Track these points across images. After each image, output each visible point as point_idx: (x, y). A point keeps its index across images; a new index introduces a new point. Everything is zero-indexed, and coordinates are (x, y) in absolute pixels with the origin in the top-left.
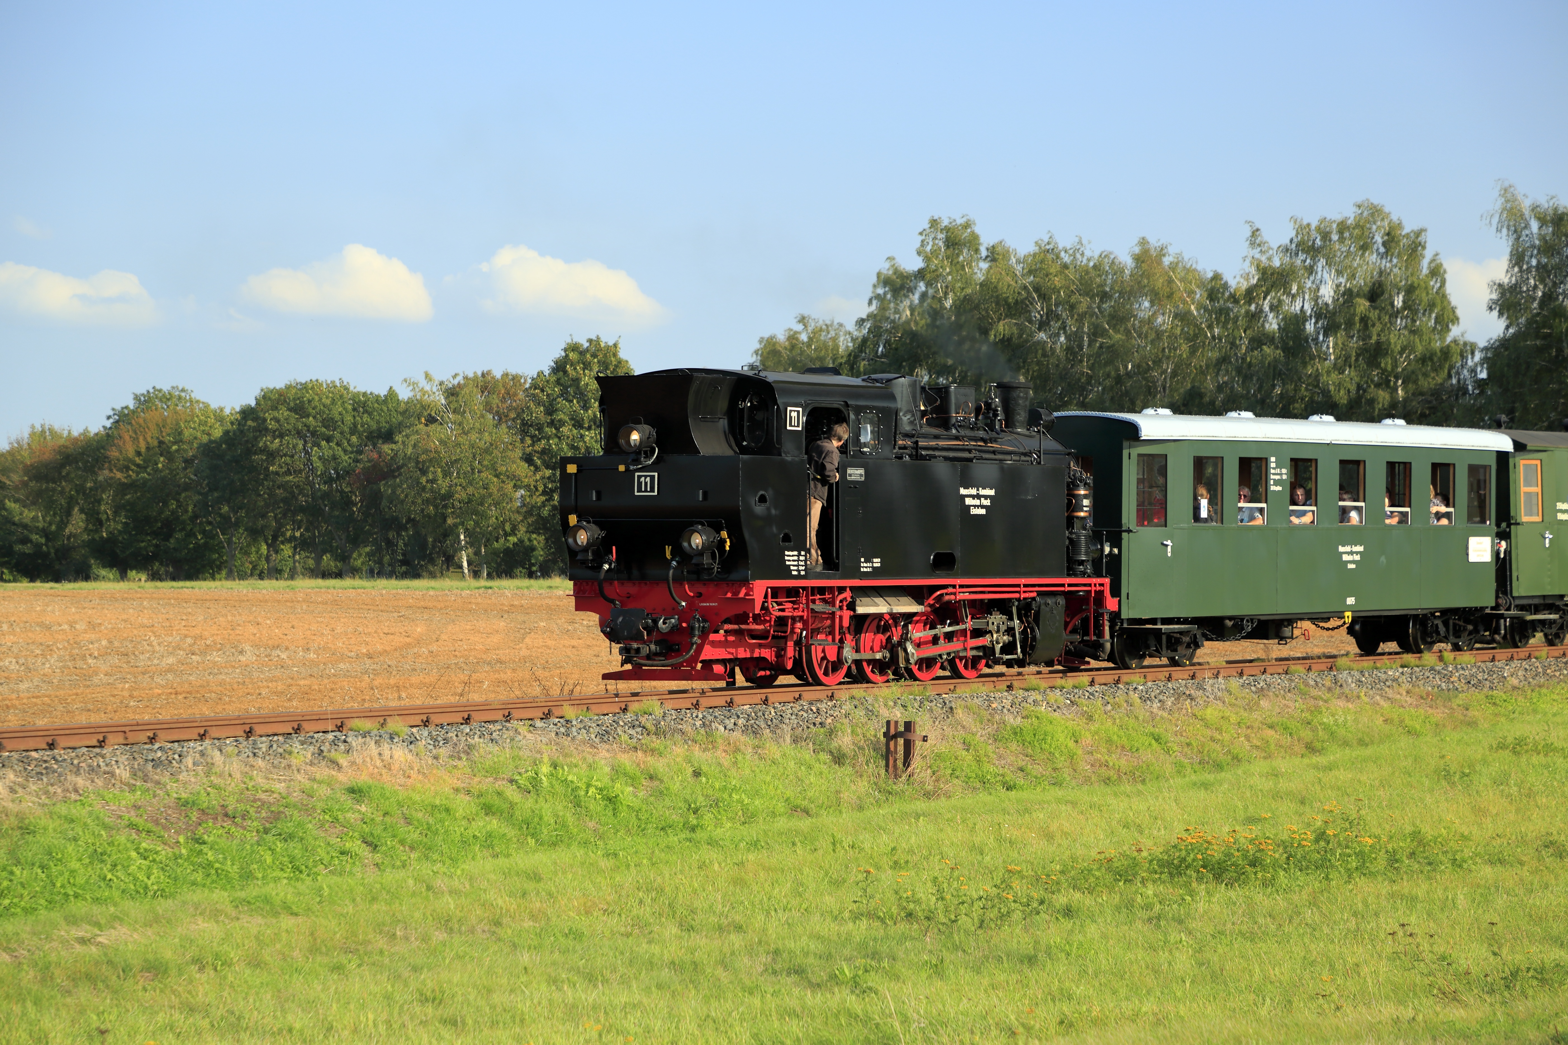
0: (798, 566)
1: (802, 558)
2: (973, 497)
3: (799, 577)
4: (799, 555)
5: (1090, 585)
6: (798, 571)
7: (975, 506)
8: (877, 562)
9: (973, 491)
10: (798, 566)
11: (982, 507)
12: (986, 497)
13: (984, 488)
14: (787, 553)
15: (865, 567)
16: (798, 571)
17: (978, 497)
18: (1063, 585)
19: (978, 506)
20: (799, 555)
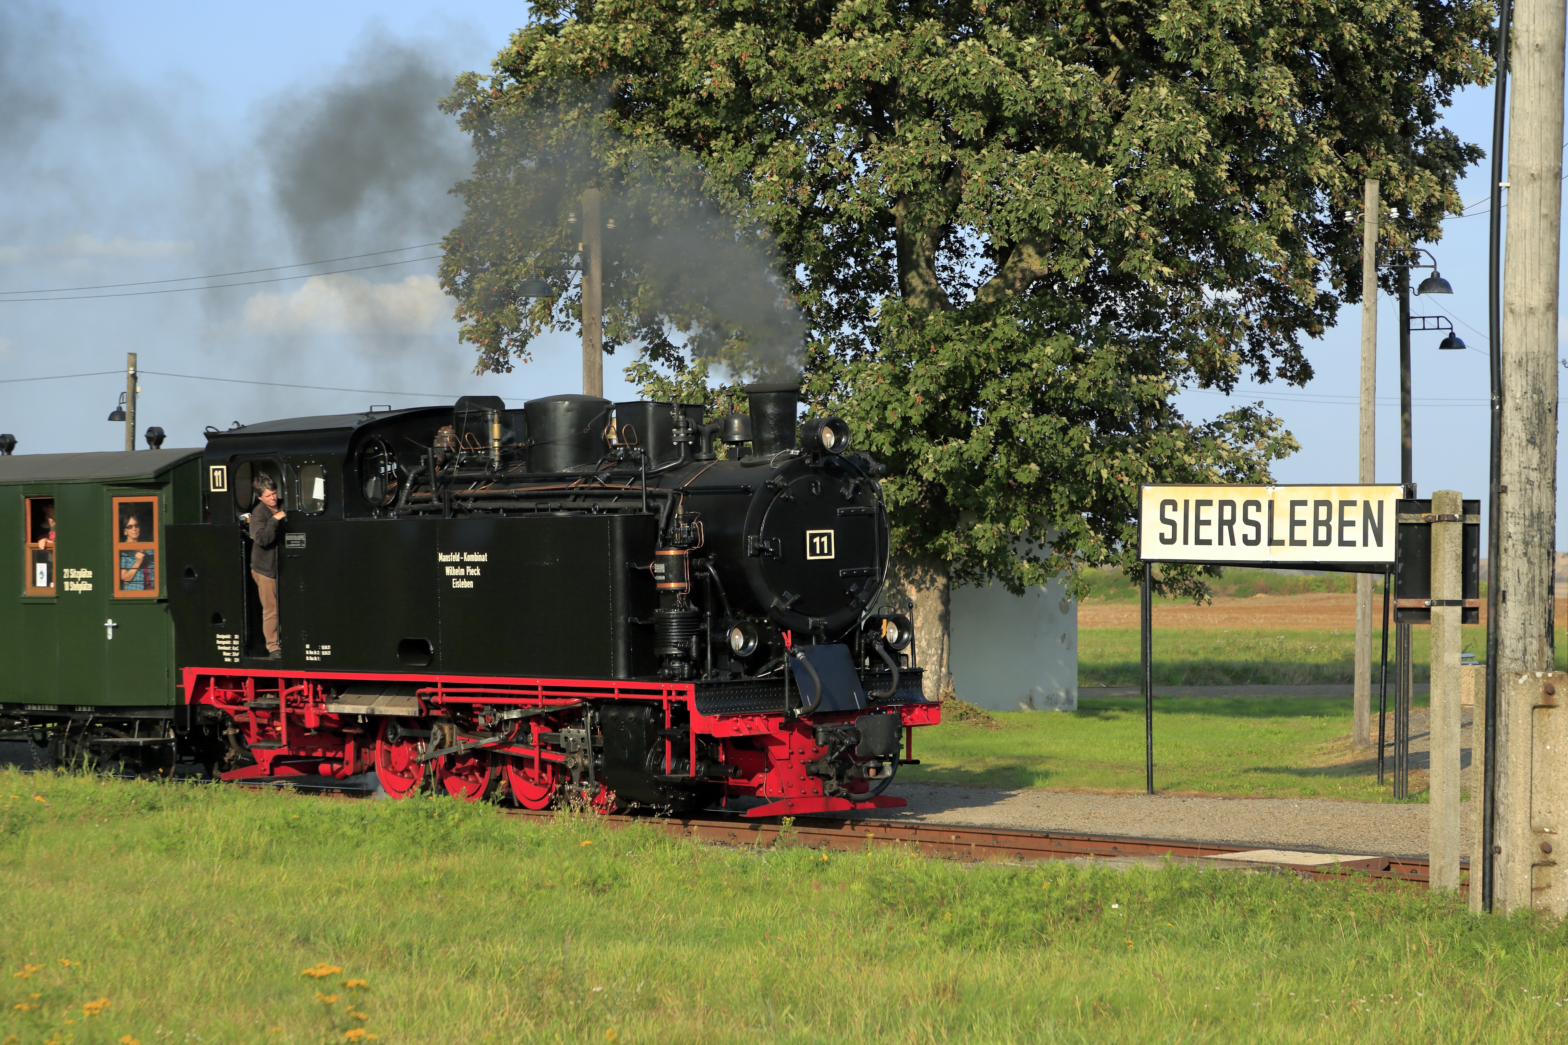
1: (236, 643)
2: (455, 565)
4: (232, 639)
5: (660, 692)
6: (232, 657)
7: (458, 577)
9: (456, 558)
11: (468, 578)
12: (473, 565)
13: (469, 553)
14: (218, 636)
15: (312, 656)
16: (232, 657)
17: (462, 564)
18: (611, 691)
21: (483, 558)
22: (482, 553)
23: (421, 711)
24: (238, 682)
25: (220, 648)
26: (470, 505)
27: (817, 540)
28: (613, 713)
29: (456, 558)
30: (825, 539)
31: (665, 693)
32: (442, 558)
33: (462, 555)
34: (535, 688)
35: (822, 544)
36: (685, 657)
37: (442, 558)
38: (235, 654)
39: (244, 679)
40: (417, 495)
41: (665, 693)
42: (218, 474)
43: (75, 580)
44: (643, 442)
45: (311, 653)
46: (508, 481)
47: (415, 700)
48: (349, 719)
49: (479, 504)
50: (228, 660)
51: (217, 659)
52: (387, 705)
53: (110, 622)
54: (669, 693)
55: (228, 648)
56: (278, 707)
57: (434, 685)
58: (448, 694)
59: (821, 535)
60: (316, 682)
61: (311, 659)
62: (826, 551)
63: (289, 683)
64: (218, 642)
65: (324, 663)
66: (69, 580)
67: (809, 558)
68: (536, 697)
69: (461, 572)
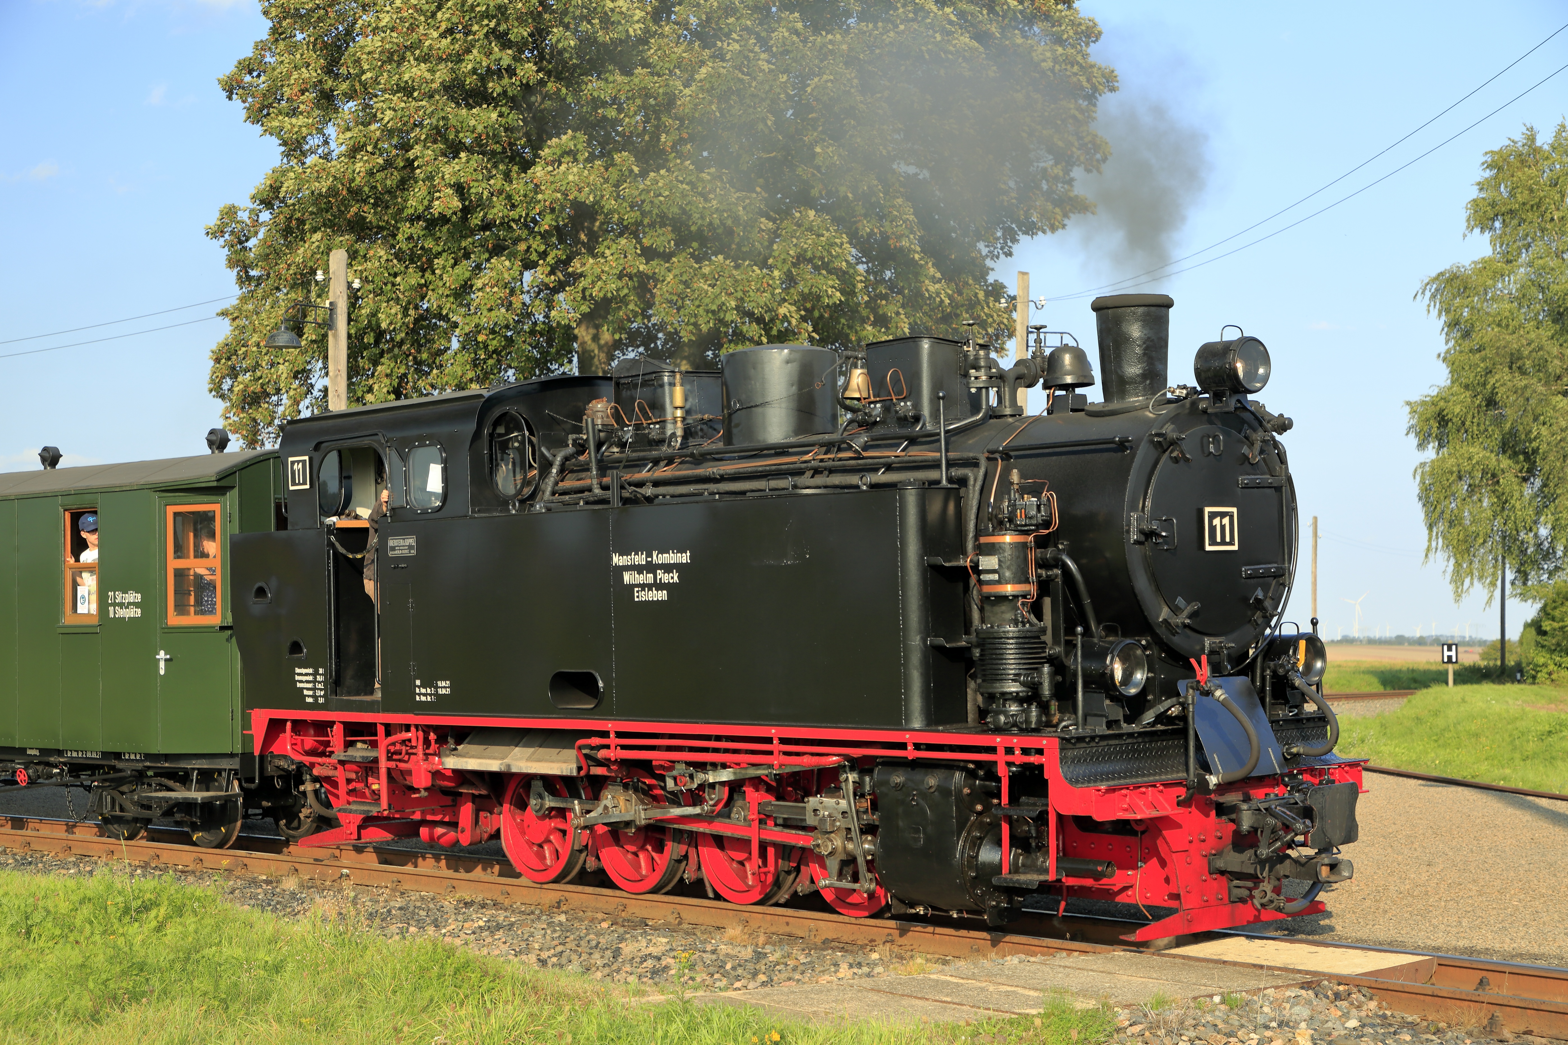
0: (314, 689)
2: (639, 569)
3: (315, 706)
4: (315, 674)
5: (992, 750)
7: (643, 586)
8: (444, 687)
9: (640, 559)
10: (314, 689)
11: (660, 586)
12: (668, 568)
13: (661, 552)
14: (298, 670)
15: (423, 694)
16: (314, 697)
17: (651, 568)
18: (903, 746)
19: (650, 587)
20: (315, 674)
21: (684, 558)
22: (682, 551)
23: (580, 769)
24: (322, 727)
25: (299, 685)
26: (649, 491)
27: (1216, 522)
28: (898, 778)
29: (640, 559)
30: (1226, 521)
31: (1001, 751)
32: (618, 560)
33: (650, 555)
34: (769, 740)
35: (1223, 527)
36: (1032, 696)
37: (618, 560)
38: (318, 693)
39: (331, 724)
40: (567, 484)
41: (1001, 751)
42: (298, 467)
43: (121, 605)
44: (914, 393)
45: (423, 691)
46: (701, 459)
47: (572, 753)
48: (463, 776)
49: (661, 490)
50: (309, 700)
51: (296, 698)
52: (529, 759)
53: (162, 655)
54: (1009, 751)
55: (310, 686)
56: (376, 760)
57: (605, 734)
58: (624, 747)
59: (1223, 515)
60: (427, 729)
61: (423, 699)
62: (1228, 540)
63: (389, 730)
64: (297, 678)
65: (440, 704)
66: (114, 605)
67: (1208, 548)
68: (770, 753)
69: (641, 579)
